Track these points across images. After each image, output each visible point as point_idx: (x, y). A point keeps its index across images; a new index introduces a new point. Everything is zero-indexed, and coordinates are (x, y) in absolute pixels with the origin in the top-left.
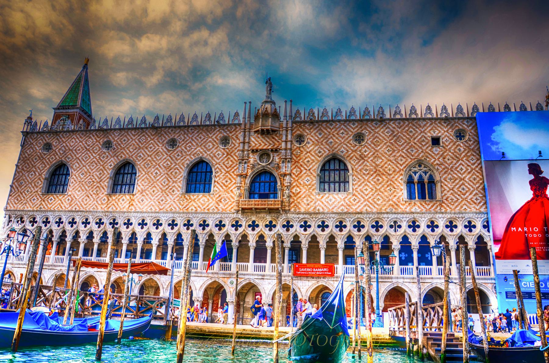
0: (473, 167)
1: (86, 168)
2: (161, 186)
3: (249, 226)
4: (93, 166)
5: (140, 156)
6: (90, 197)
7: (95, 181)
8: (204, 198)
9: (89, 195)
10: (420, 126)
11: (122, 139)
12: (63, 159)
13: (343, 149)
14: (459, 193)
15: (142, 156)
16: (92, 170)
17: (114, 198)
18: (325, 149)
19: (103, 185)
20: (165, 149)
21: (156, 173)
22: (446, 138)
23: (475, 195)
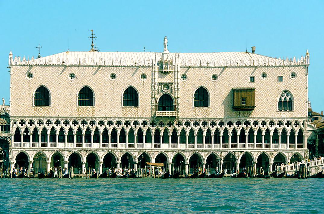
0: (268, 94)
1: (60, 90)
2: (110, 102)
3: (159, 124)
4: (65, 89)
5: (94, 84)
6: (67, 108)
7: (68, 99)
8: (135, 109)
9: (66, 107)
10: (244, 70)
11: (80, 72)
12: (43, 84)
13: (206, 83)
14: (260, 107)
15: (96, 84)
16: (65, 92)
17: (82, 109)
18: (197, 83)
19: (73, 101)
20: (109, 80)
21: (106, 95)
22: (257, 77)
23: (267, 109)
